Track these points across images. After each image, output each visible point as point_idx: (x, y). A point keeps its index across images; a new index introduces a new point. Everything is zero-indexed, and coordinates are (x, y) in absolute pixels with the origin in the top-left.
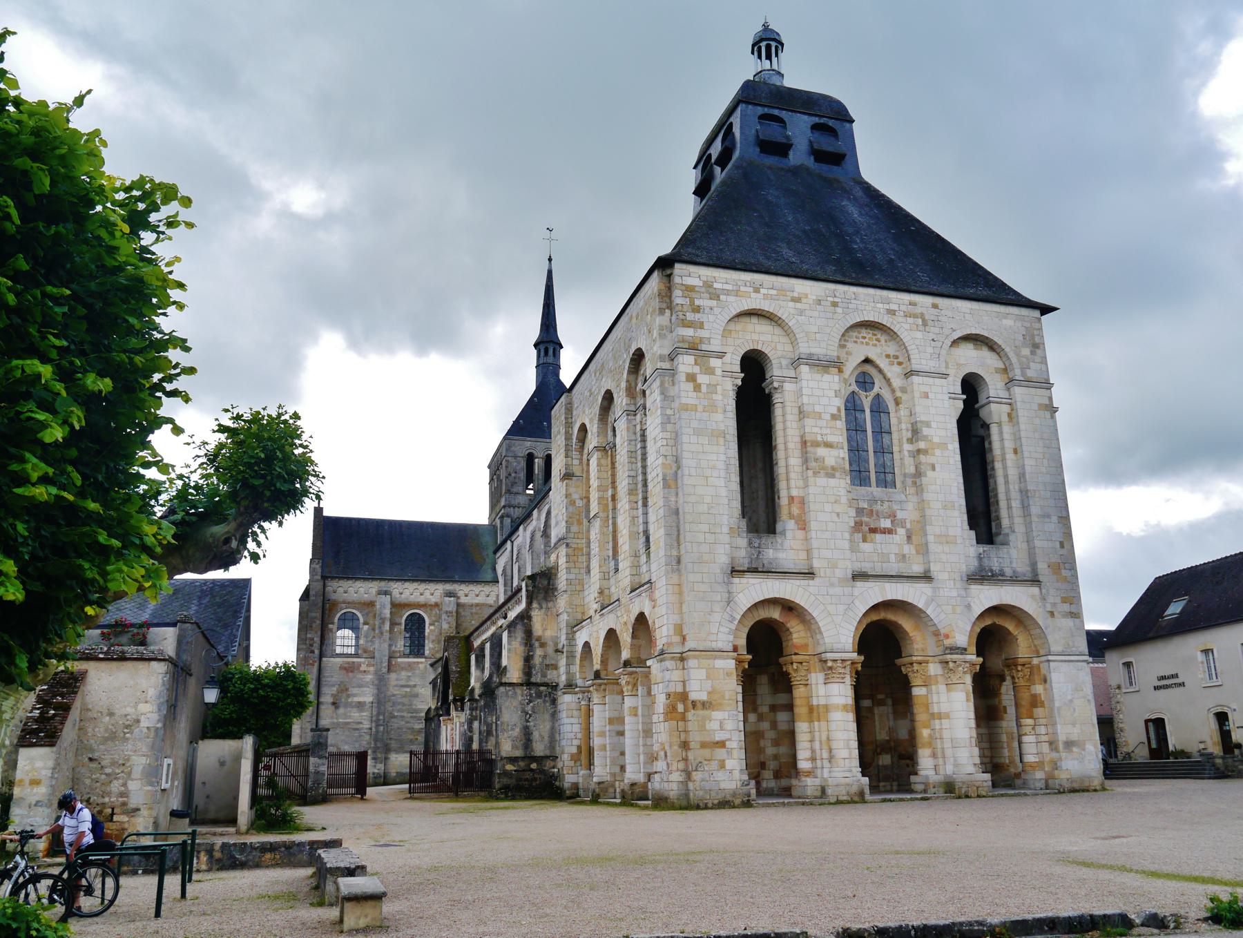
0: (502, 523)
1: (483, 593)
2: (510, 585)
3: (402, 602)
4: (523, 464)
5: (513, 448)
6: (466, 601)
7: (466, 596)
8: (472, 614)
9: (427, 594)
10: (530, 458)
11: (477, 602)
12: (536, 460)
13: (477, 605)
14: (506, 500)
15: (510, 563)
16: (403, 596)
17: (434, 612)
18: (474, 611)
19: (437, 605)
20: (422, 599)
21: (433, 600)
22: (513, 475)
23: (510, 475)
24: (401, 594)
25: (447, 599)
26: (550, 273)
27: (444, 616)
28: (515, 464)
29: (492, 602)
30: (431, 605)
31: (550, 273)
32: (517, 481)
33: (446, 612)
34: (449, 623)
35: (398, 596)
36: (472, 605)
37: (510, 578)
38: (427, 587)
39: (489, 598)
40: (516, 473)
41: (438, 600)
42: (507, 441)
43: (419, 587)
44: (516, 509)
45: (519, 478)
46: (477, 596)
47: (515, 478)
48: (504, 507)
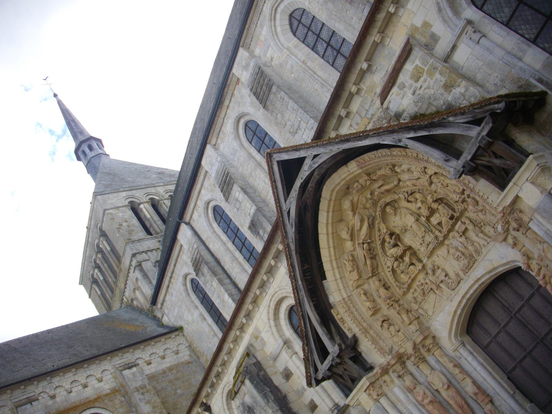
0: (142, 270)
1: (168, 352)
2: (220, 271)
3: (62, 409)
4: (129, 213)
5: (109, 202)
6: (153, 370)
7: (149, 364)
8: (170, 381)
9: (93, 382)
10: (135, 209)
11: (168, 365)
12: (142, 206)
13: (170, 369)
14: (132, 249)
15: (202, 247)
16: (58, 399)
17: (117, 402)
18: (171, 377)
19: (115, 391)
20: (89, 393)
21: (107, 386)
22: (125, 224)
23: (121, 225)
24: (53, 397)
25: (126, 372)
26: (60, 103)
27: (137, 396)
28: (120, 214)
29: (187, 358)
30: (107, 395)
31: (60, 103)
32: (132, 228)
33: (137, 389)
34: (148, 402)
35: (50, 402)
36: (164, 372)
37: (213, 263)
38: (88, 373)
39: (180, 355)
40: (126, 221)
41: (114, 385)
42: (99, 197)
43: (76, 378)
44: (149, 253)
45: (133, 225)
46: (163, 358)
47: (129, 226)
48: (134, 255)
